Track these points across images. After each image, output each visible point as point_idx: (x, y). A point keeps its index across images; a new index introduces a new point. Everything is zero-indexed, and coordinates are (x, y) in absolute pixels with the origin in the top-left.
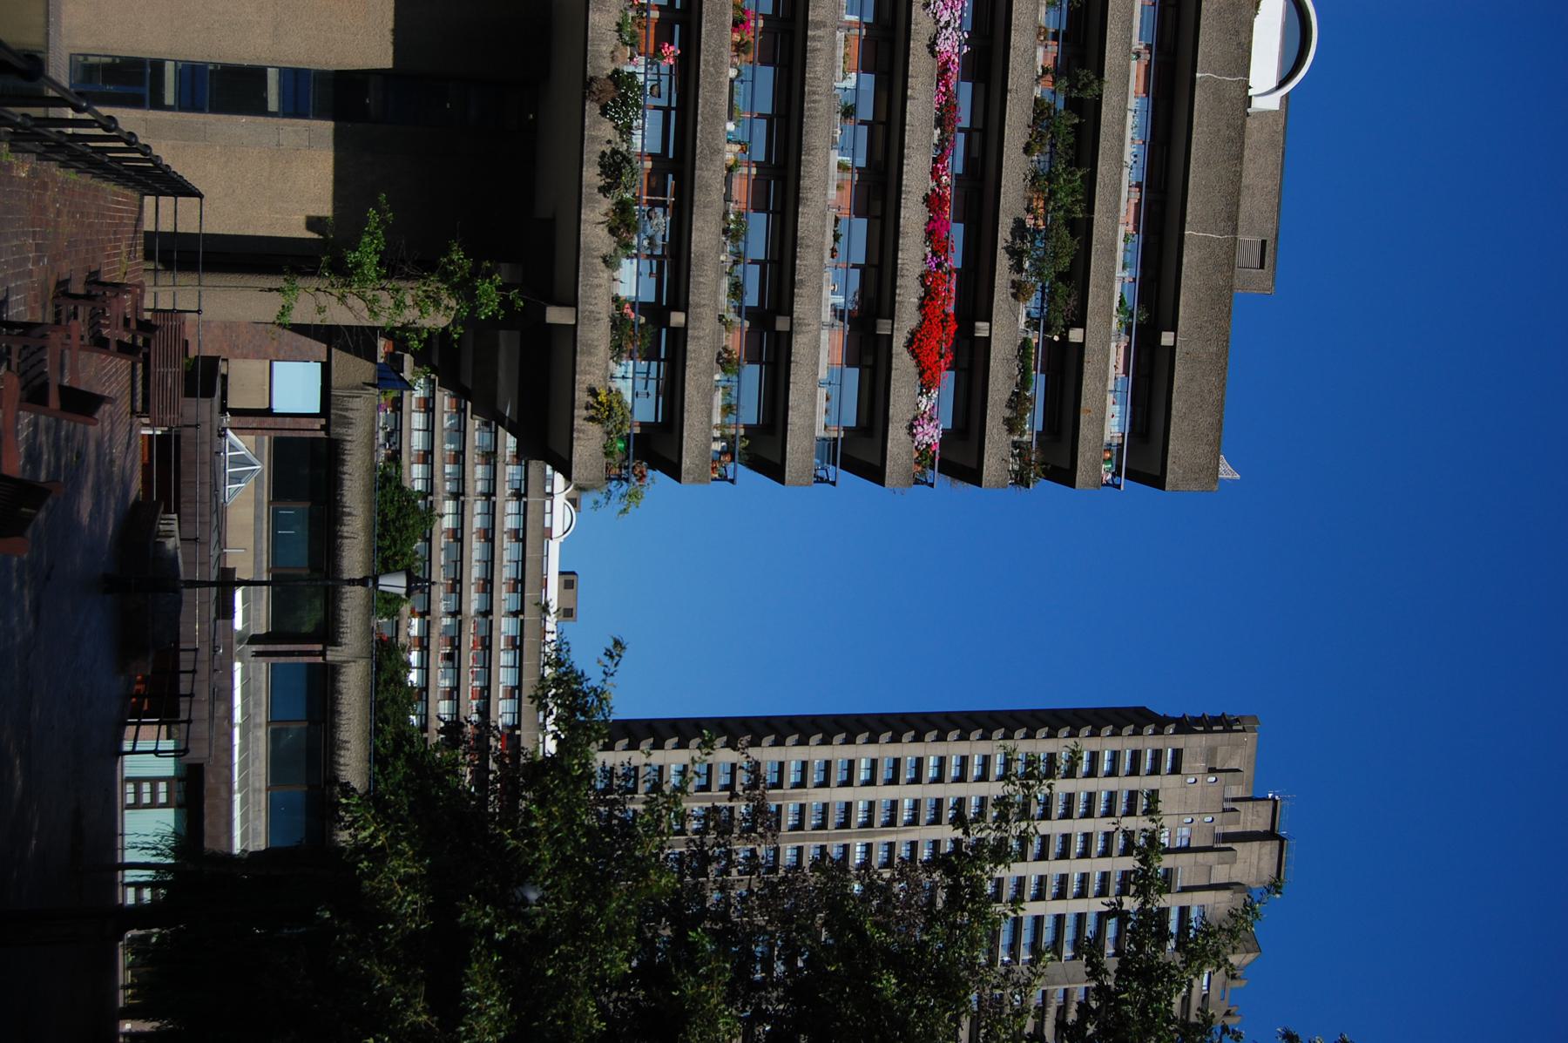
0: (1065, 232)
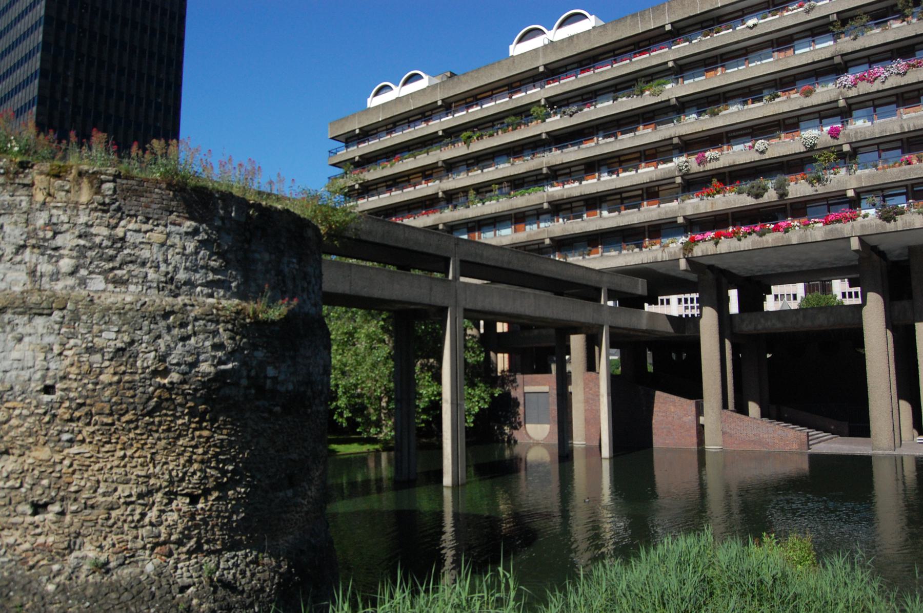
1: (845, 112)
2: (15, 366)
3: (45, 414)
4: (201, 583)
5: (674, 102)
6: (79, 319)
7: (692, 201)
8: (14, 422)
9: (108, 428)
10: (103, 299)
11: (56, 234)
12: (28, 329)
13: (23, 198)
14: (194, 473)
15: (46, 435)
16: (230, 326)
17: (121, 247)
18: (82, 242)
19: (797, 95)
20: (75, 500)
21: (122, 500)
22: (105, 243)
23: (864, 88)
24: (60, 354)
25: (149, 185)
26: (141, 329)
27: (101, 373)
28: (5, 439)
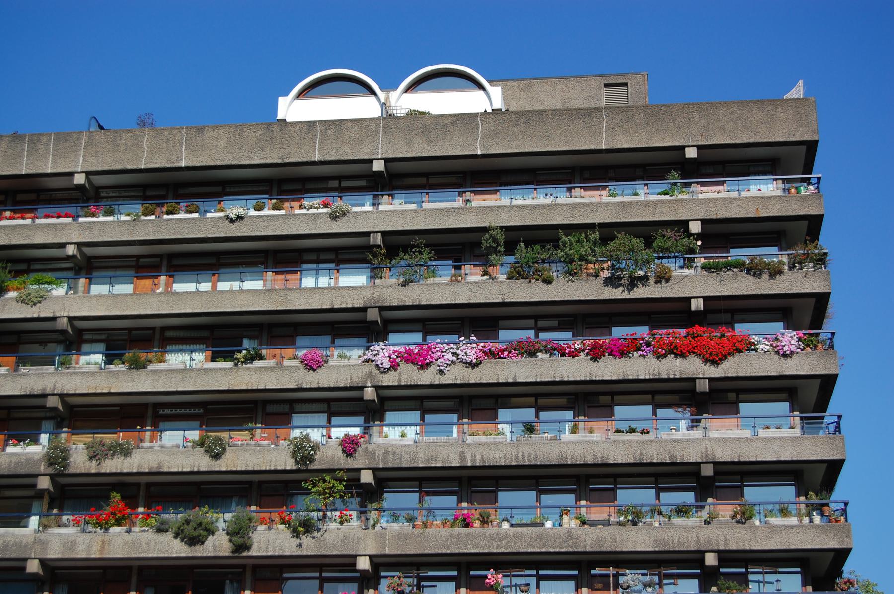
0: (612, 245)
1: (372, 408)
5: (63, 323)
7: (63, 530)
19: (296, 363)
23: (409, 375)
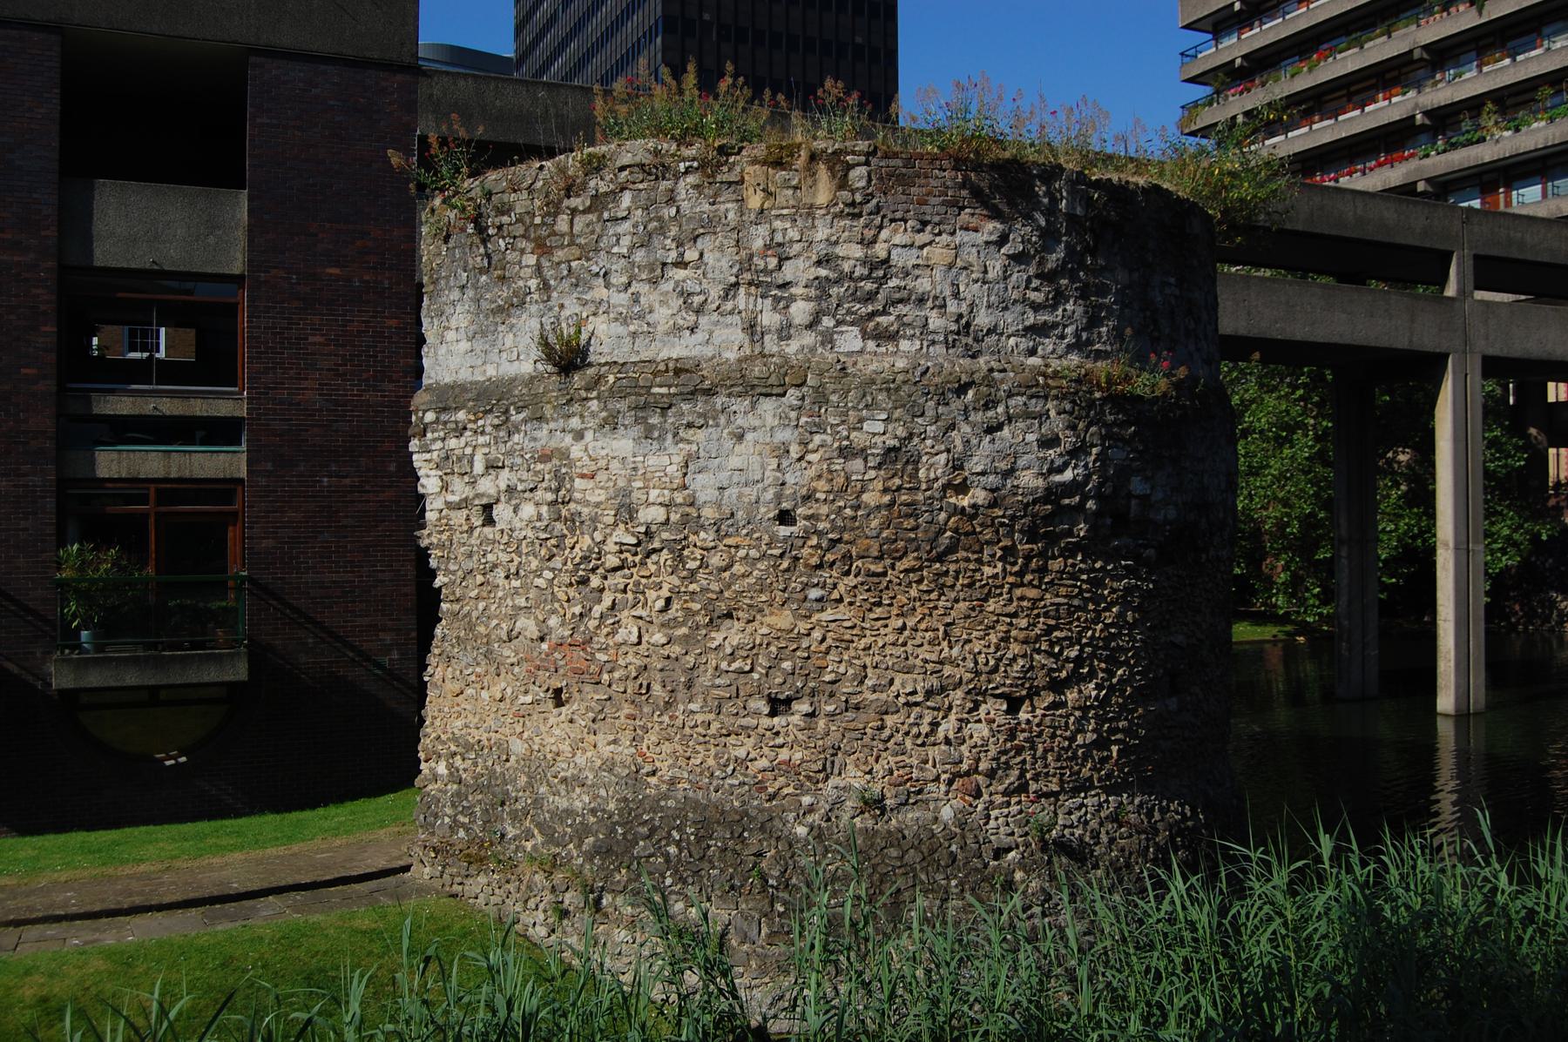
2: (735, 480)
3: (782, 556)
4: (1027, 845)
6: (827, 401)
8: (738, 568)
9: (876, 580)
10: (860, 365)
11: (782, 260)
12: (752, 421)
13: (729, 205)
14: (1014, 659)
15: (784, 591)
16: (1068, 407)
17: (885, 275)
18: (823, 272)
20: (832, 695)
21: (902, 700)
22: (859, 271)
24: (800, 459)
25: (924, 164)
26: (922, 415)
27: (863, 491)
28: (726, 594)
